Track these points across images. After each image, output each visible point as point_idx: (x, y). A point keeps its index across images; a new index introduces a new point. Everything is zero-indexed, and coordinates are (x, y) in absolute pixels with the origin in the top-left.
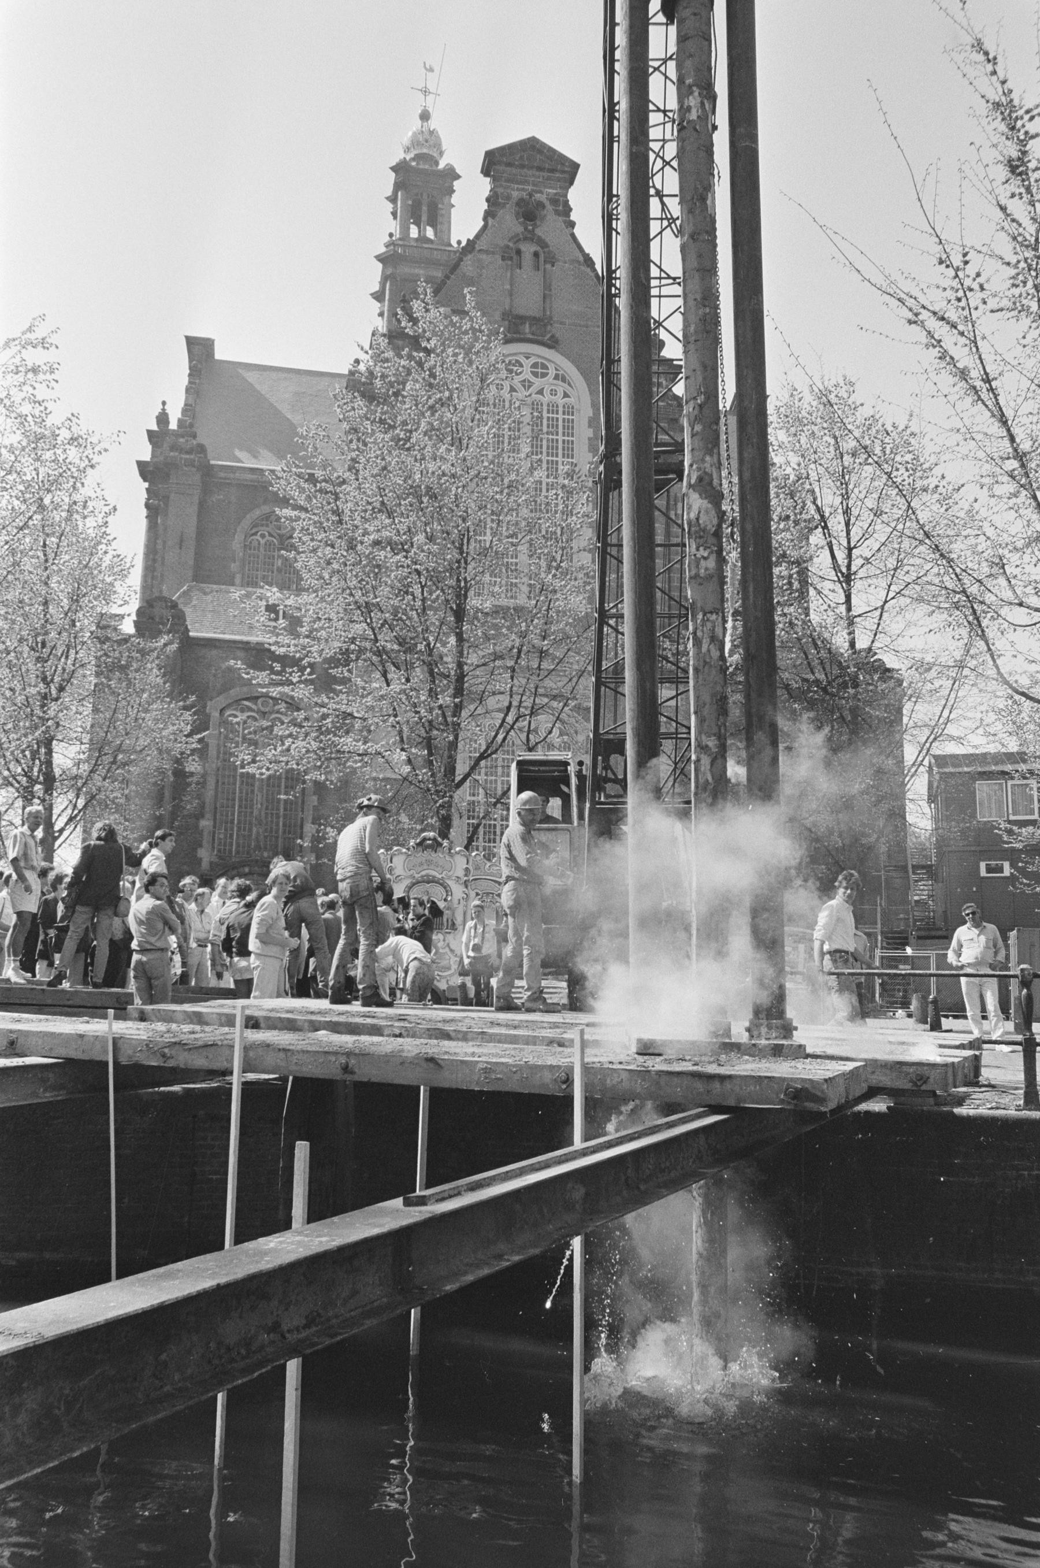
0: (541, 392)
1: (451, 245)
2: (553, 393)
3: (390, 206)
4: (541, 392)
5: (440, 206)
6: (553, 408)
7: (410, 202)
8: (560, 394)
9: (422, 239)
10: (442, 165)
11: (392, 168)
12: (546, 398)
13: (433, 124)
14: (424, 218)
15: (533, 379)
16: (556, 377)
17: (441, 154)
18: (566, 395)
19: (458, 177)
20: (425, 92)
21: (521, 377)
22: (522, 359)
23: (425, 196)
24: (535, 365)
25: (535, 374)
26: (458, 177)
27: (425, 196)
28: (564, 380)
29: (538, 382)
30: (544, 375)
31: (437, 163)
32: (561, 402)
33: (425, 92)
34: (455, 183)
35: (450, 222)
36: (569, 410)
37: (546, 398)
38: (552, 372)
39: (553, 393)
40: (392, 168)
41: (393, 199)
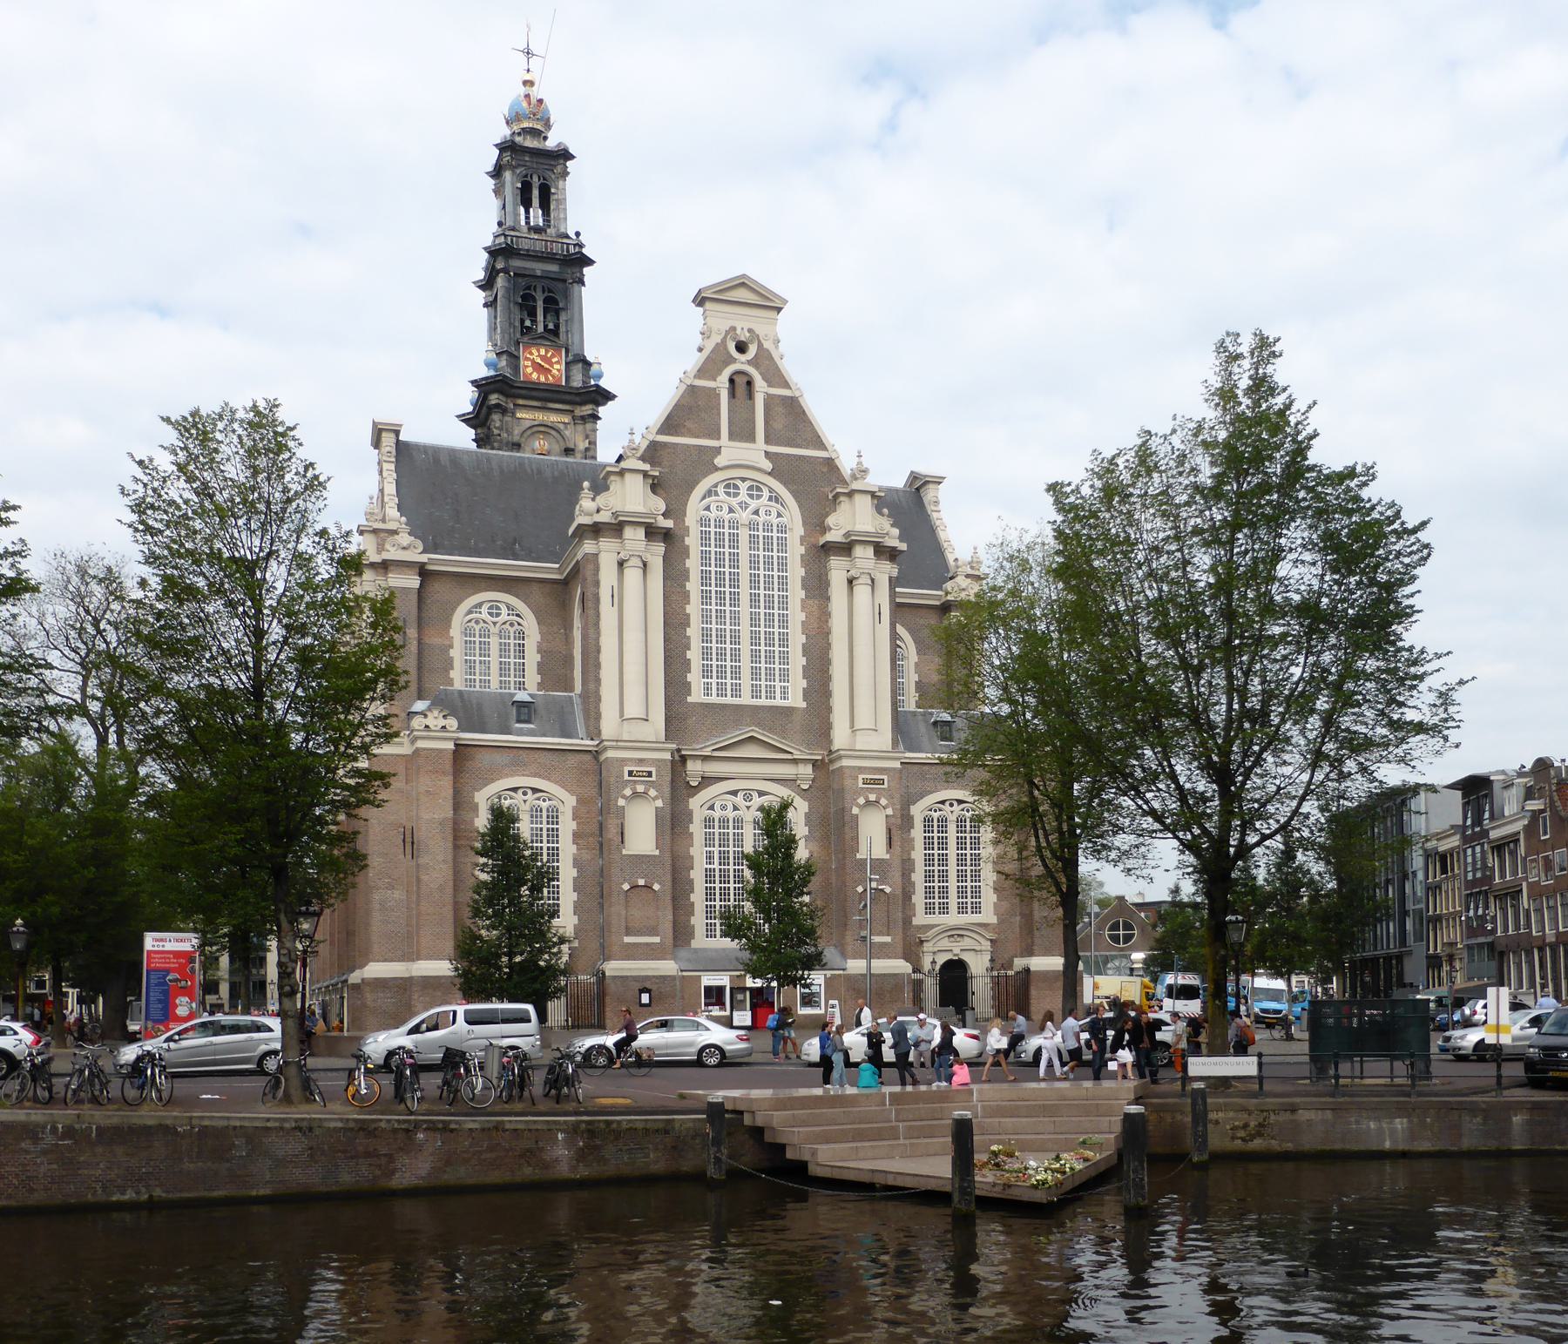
0: (756, 512)
1: (567, 237)
2: (768, 513)
3: (491, 183)
4: (756, 512)
5: (553, 190)
6: (768, 527)
7: (519, 185)
8: (774, 514)
9: (537, 230)
10: (551, 143)
11: (496, 145)
12: (762, 519)
13: (536, 93)
14: (536, 201)
15: (748, 500)
16: (770, 499)
17: (548, 125)
18: (779, 515)
19: (571, 157)
20: (528, 53)
21: (739, 499)
22: (739, 483)
23: (535, 179)
24: (750, 488)
25: (751, 496)
26: (571, 157)
27: (535, 179)
28: (777, 501)
29: (754, 504)
30: (759, 497)
31: (545, 138)
32: (775, 521)
33: (528, 53)
34: (568, 163)
35: (565, 209)
36: (782, 529)
37: (762, 519)
38: (766, 493)
39: (768, 513)
40: (496, 145)
41: (497, 173)
